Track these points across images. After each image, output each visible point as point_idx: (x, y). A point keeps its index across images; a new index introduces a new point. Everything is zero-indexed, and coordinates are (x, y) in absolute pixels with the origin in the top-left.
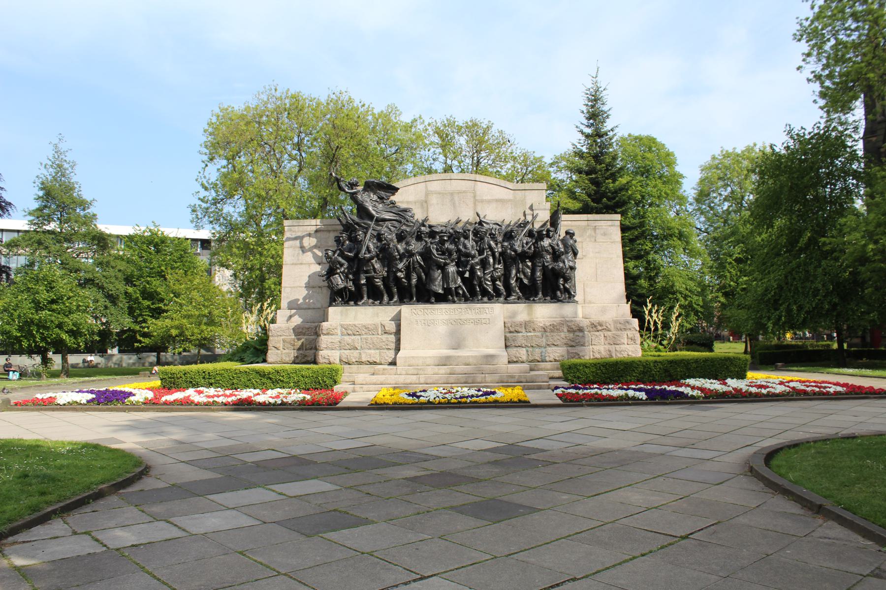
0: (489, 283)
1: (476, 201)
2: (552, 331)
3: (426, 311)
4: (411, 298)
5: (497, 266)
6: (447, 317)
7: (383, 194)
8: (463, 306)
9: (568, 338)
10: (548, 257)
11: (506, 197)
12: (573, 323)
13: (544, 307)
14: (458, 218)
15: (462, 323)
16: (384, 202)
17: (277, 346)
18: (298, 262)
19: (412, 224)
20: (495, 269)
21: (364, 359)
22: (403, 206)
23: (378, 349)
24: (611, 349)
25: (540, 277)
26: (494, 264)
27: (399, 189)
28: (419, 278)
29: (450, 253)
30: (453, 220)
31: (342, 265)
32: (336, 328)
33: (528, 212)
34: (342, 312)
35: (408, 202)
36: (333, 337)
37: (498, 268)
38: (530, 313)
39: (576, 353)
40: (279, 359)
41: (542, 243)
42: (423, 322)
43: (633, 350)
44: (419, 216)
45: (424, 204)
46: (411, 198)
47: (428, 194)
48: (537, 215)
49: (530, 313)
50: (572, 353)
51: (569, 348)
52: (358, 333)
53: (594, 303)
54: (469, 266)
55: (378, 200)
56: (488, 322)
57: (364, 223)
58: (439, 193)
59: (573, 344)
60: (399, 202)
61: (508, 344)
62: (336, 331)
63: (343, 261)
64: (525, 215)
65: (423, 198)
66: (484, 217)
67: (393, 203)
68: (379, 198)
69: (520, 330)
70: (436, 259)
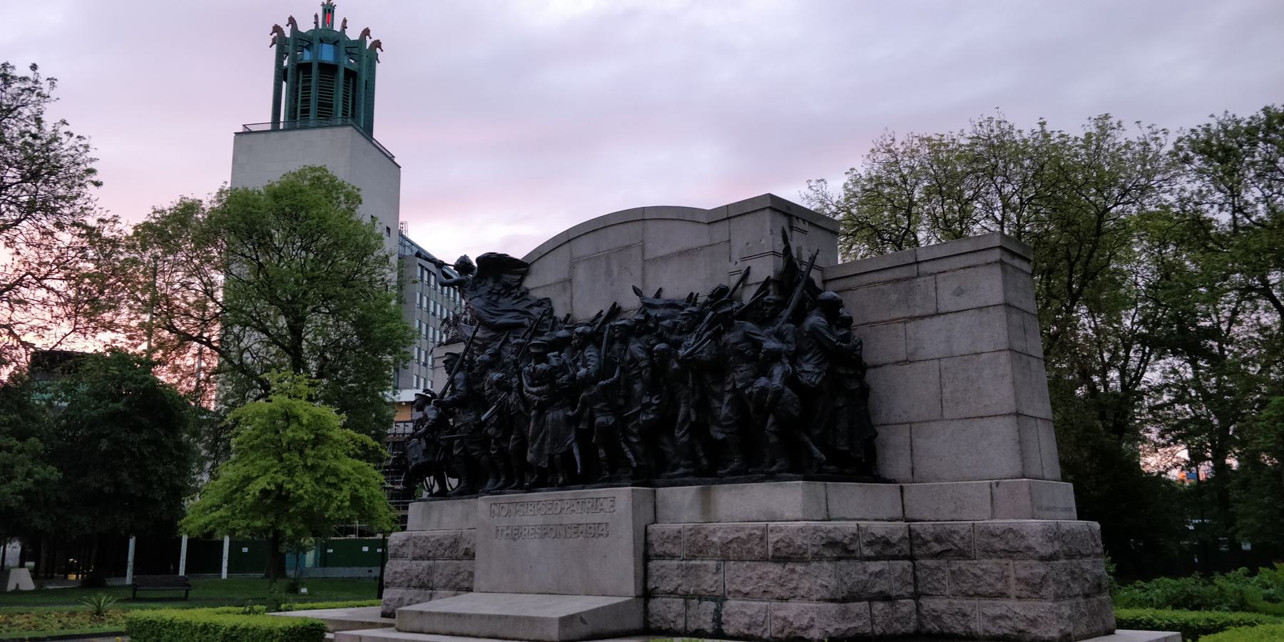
0: (635, 440)
4: (522, 481)
6: (539, 520)
9: (772, 576)
10: (744, 367)
11: (696, 243)
12: (781, 535)
13: (733, 491)
14: (615, 304)
16: (510, 294)
22: (539, 295)
24: (968, 610)
25: (730, 419)
32: (404, 545)
36: (400, 561)
37: (649, 405)
38: (706, 506)
39: (784, 619)
43: (1031, 615)
47: (572, 266)
49: (706, 506)
51: (775, 604)
53: (939, 480)
58: (589, 259)
59: (779, 591)
61: (651, 585)
62: (404, 550)
65: (566, 276)
66: (658, 295)
67: (527, 291)
69: (675, 551)
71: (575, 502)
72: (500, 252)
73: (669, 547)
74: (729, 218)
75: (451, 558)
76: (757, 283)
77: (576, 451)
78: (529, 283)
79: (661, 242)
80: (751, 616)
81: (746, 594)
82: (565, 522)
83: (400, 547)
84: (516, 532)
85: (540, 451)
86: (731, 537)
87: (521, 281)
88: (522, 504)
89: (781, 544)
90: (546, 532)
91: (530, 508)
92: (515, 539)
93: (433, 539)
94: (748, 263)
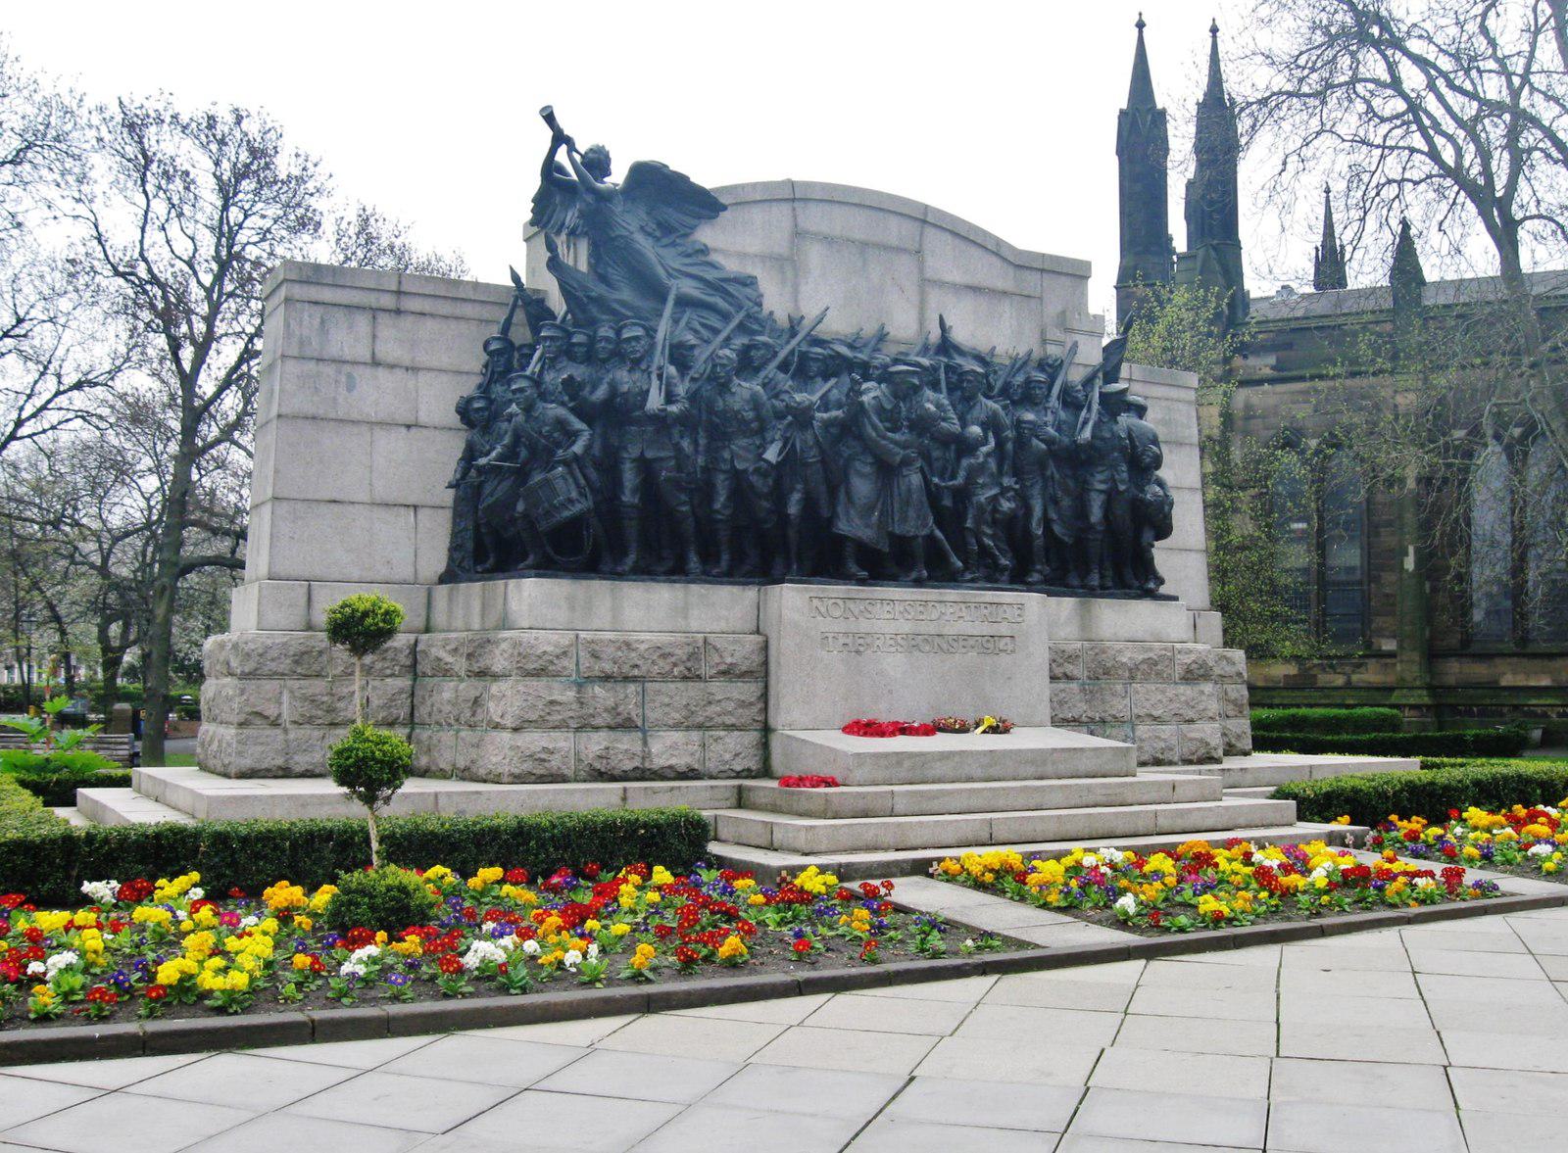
1: (925, 283)
2: (1146, 679)
3: (851, 605)
5: (1007, 481)
6: (906, 627)
7: (672, 216)
8: (951, 594)
9: (1183, 698)
11: (1000, 285)
12: (1193, 657)
15: (945, 646)
16: (673, 244)
17: (271, 711)
18: (332, 415)
19: (756, 327)
20: (1004, 491)
21: (659, 762)
22: (732, 266)
23: (700, 727)
26: (1000, 472)
27: (724, 208)
28: (809, 503)
29: (922, 425)
30: (869, 330)
31: (576, 434)
32: (565, 653)
33: (1054, 334)
34: (571, 601)
35: (743, 256)
37: (1009, 489)
39: (1201, 740)
40: (280, 761)
41: (1115, 428)
42: (842, 640)
44: (776, 302)
45: (788, 264)
46: (753, 244)
48: (1075, 345)
49: (1085, 621)
50: (1191, 739)
51: (1184, 727)
52: (636, 672)
54: (962, 474)
55: (658, 234)
56: (1010, 647)
57: (619, 302)
59: (1190, 714)
60: (716, 250)
62: (565, 662)
63: (578, 424)
64: (1044, 342)
68: (659, 224)
70: (884, 442)
71: (963, 606)
72: (676, 165)
73: (1069, 668)
74: (1042, 271)
75: (685, 678)
76: (1086, 366)
77: (938, 534)
78: (707, 235)
79: (946, 262)
80: (1165, 740)
81: (1155, 719)
82: (945, 631)
83: (557, 657)
84: (861, 641)
85: (882, 524)
86: (1141, 657)
87: (693, 228)
88: (872, 601)
89: (1194, 666)
90: (914, 643)
91: (888, 608)
92: (858, 652)
93: (643, 647)
94: (1080, 339)
